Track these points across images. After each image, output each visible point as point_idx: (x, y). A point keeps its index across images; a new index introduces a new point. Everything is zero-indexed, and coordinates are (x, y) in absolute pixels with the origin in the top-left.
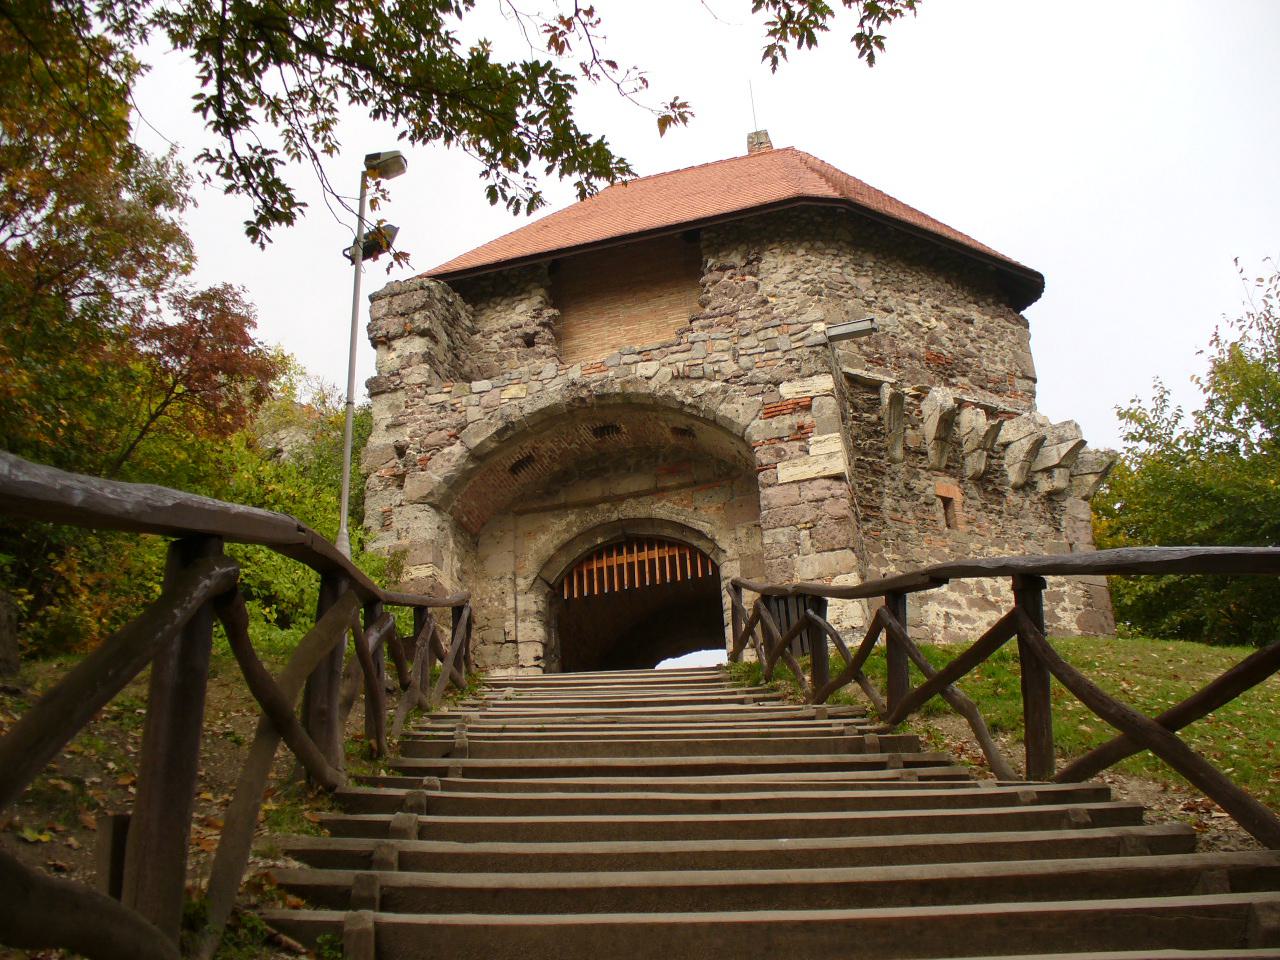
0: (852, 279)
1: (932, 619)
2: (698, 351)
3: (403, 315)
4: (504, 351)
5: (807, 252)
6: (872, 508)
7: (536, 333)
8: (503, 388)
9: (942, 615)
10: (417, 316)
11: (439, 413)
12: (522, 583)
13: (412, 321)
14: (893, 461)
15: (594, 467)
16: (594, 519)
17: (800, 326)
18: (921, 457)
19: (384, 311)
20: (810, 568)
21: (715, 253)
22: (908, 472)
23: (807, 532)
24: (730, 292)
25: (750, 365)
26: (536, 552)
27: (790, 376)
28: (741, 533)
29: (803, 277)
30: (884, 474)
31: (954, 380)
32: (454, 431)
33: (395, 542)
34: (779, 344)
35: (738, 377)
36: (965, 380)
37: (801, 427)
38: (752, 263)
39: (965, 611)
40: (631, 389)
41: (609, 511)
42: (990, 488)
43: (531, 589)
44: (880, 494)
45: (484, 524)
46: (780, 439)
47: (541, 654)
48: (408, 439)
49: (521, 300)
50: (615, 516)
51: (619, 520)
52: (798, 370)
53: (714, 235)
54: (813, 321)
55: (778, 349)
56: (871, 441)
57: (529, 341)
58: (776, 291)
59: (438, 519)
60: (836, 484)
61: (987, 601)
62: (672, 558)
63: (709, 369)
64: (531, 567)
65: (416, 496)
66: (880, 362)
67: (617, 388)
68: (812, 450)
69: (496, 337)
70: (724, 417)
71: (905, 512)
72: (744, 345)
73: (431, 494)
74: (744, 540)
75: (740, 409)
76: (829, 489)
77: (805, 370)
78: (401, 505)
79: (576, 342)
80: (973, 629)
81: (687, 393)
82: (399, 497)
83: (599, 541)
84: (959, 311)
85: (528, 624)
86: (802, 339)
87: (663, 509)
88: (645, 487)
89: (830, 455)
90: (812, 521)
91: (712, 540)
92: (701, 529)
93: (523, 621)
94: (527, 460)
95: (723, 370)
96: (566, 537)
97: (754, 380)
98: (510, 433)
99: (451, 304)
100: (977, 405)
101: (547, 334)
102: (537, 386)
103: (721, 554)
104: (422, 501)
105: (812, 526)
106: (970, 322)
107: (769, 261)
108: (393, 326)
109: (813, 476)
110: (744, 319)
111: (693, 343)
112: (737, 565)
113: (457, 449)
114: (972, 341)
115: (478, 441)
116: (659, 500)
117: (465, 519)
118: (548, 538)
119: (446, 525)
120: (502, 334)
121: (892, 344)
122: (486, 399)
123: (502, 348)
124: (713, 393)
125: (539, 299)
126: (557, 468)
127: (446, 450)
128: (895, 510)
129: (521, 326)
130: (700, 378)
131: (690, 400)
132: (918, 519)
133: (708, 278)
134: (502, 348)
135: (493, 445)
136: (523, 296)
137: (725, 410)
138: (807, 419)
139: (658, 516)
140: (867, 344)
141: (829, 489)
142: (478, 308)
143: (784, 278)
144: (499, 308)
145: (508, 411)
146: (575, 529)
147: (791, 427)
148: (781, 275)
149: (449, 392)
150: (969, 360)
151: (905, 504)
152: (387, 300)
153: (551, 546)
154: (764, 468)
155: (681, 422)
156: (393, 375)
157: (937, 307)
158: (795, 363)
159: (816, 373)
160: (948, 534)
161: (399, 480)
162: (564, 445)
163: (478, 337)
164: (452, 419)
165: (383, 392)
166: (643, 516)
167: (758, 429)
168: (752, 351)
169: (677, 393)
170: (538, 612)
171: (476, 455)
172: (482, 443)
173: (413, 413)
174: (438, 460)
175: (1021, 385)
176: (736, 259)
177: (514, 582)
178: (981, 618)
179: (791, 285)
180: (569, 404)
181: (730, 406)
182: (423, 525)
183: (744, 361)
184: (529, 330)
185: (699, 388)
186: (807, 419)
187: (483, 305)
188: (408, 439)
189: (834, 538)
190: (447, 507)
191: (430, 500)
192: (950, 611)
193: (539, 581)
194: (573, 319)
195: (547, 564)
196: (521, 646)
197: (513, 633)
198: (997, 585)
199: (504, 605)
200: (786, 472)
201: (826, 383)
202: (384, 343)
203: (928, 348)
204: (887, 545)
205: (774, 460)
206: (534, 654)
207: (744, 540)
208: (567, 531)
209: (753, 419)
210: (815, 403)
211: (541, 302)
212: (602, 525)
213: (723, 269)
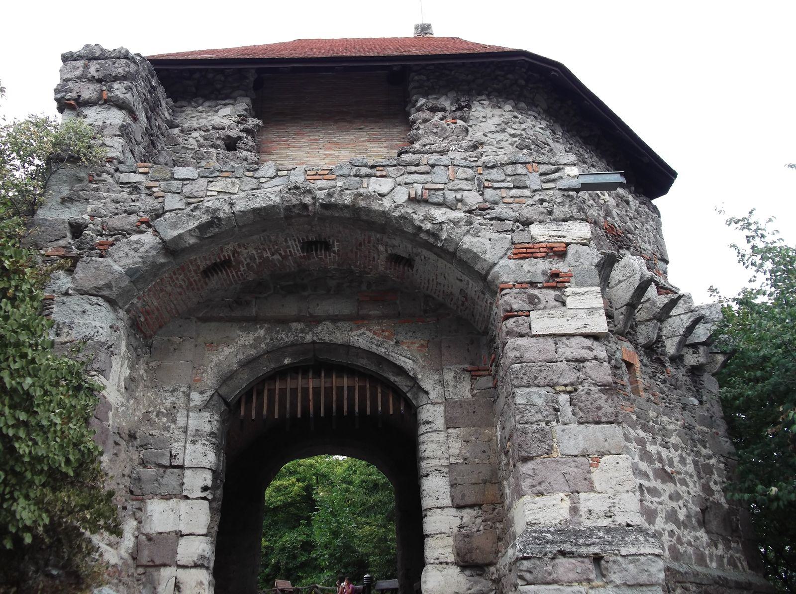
2: (440, 175)
3: (99, 81)
4: (202, 149)
7: (240, 138)
10: (116, 85)
11: (130, 193)
12: (197, 398)
13: (110, 89)
15: (291, 283)
16: (285, 337)
19: (78, 73)
20: (572, 442)
21: (426, 95)
23: (567, 396)
24: (440, 133)
25: (497, 198)
26: (216, 365)
27: (541, 218)
28: (449, 376)
32: (146, 217)
34: (528, 183)
35: (484, 209)
37: (556, 275)
38: (462, 108)
40: (362, 204)
41: (302, 331)
43: (206, 406)
45: (160, 327)
46: (533, 284)
47: (209, 483)
48: (86, 217)
49: (225, 105)
50: (309, 338)
51: (314, 342)
53: (424, 78)
54: (565, 164)
55: (526, 187)
58: (484, 139)
59: (112, 316)
60: (596, 345)
61: (666, 472)
62: (362, 389)
64: (209, 379)
65: (88, 286)
67: (347, 199)
68: (569, 301)
69: (195, 134)
70: (468, 251)
73: (108, 286)
74: (452, 384)
75: (486, 244)
77: (558, 212)
78: (66, 294)
80: (660, 503)
81: (425, 218)
83: (286, 362)
85: (199, 447)
87: (363, 338)
88: (346, 311)
89: (591, 311)
90: (572, 384)
91: (414, 379)
92: (402, 364)
93: (193, 442)
94: (223, 265)
95: (467, 200)
96: (253, 352)
97: (503, 216)
99: (154, 88)
102: (253, 183)
103: (421, 395)
104: (95, 292)
105: (572, 390)
108: (88, 92)
109: (573, 331)
111: (433, 166)
112: (440, 409)
114: (631, 219)
115: (176, 233)
116: (359, 328)
117: (142, 319)
118: (232, 351)
119: (120, 324)
120: (203, 133)
123: (200, 146)
124: (456, 223)
125: (245, 106)
126: (251, 277)
127: (134, 238)
129: (223, 129)
130: (439, 205)
131: (428, 226)
134: (200, 146)
135: (192, 241)
136: (227, 101)
137: (468, 242)
139: (356, 345)
141: (591, 349)
142: (179, 104)
143: (493, 128)
144: (200, 108)
146: (263, 346)
147: (544, 273)
149: (146, 173)
153: (235, 361)
154: (510, 314)
155: (403, 248)
158: (545, 204)
159: (572, 218)
160: (634, 400)
162: (266, 254)
163: (176, 131)
164: (146, 203)
166: (340, 341)
167: (507, 270)
168: (496, 185)
170: (212, 434)
171: (170, 249)
172: (180, 236)
173: (97, 190)
174: (122, 246)
175: (660, 264)
179: (500, 136)
181: (476, 240)
183: (489, 193)
184: (234, 133)
186: (561, 267)
187: (183, 103)
188: (86, 217)
190: (125, 303)
191: (106, 293)
192: (643, 482)
193: (216, 397)
194: (272, 136)
195: (226, 379)
196: (188, 473)
197: (180, 457)
200: (540, 323)
201: (581, 230)
202: (72, 108)
203: (605, 218)
205: (527, 307)
206: (202, 484)
207: (452, 384)
209: (501, 258)
210: (571, 250)
211: (246, 110)
212: (293, 345)
213: (434, 110)
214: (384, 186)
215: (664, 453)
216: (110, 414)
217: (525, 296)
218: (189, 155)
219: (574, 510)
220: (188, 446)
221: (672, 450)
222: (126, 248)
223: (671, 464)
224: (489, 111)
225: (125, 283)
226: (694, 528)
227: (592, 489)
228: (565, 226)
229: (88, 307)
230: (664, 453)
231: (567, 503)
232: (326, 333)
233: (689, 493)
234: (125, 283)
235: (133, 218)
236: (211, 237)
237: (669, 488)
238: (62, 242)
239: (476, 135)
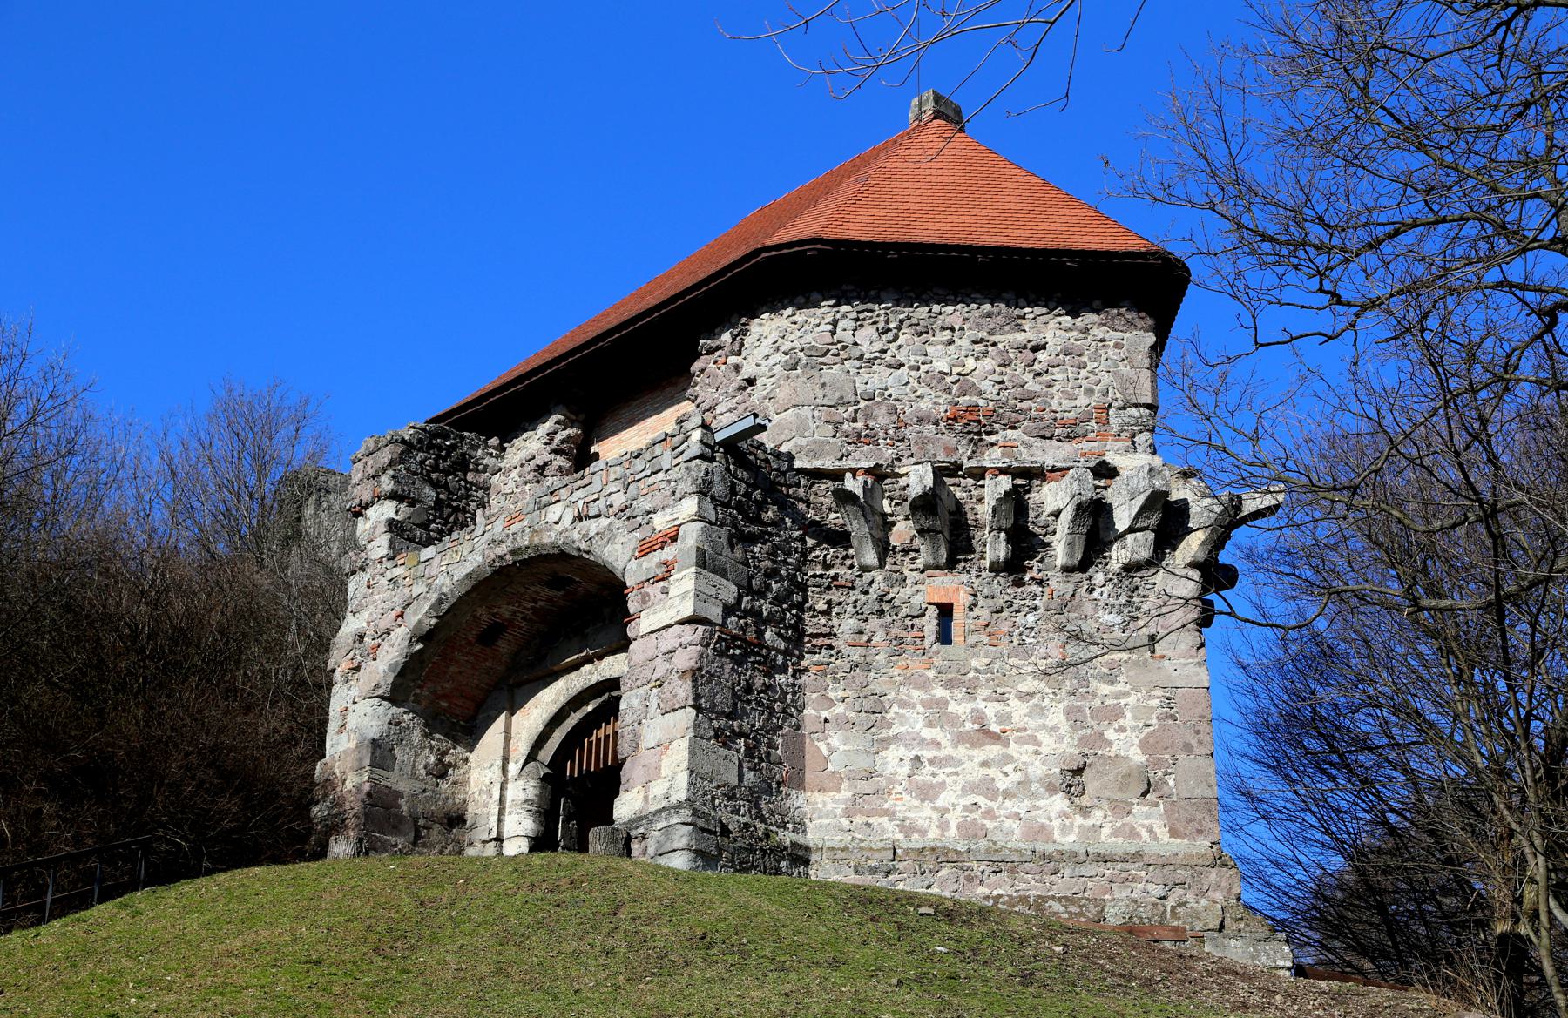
18: (913, 555)
29: (786, 346)
31: (993, 438)
39: (948, 751)
66: (872, 439)
69: (514, 474)
73: (377, 687)
101: (560, 461)
133: (695, 367)
150: (1026, 404)
162: (530, 605)
167: (633, 573)
178: (971, 758)
185: (593, 527)
191: (380, 692)
198: (1007, 709)
204: (836, 680)
213: (711, 351)
215: (991, 710)
216: (402, 802)
219: (646, 798)
221: (1014, 702)
223: (1004, 718)
226: (1034, 795)
230: (991, 710)
233: (1037, 753)
237: (993, 751)
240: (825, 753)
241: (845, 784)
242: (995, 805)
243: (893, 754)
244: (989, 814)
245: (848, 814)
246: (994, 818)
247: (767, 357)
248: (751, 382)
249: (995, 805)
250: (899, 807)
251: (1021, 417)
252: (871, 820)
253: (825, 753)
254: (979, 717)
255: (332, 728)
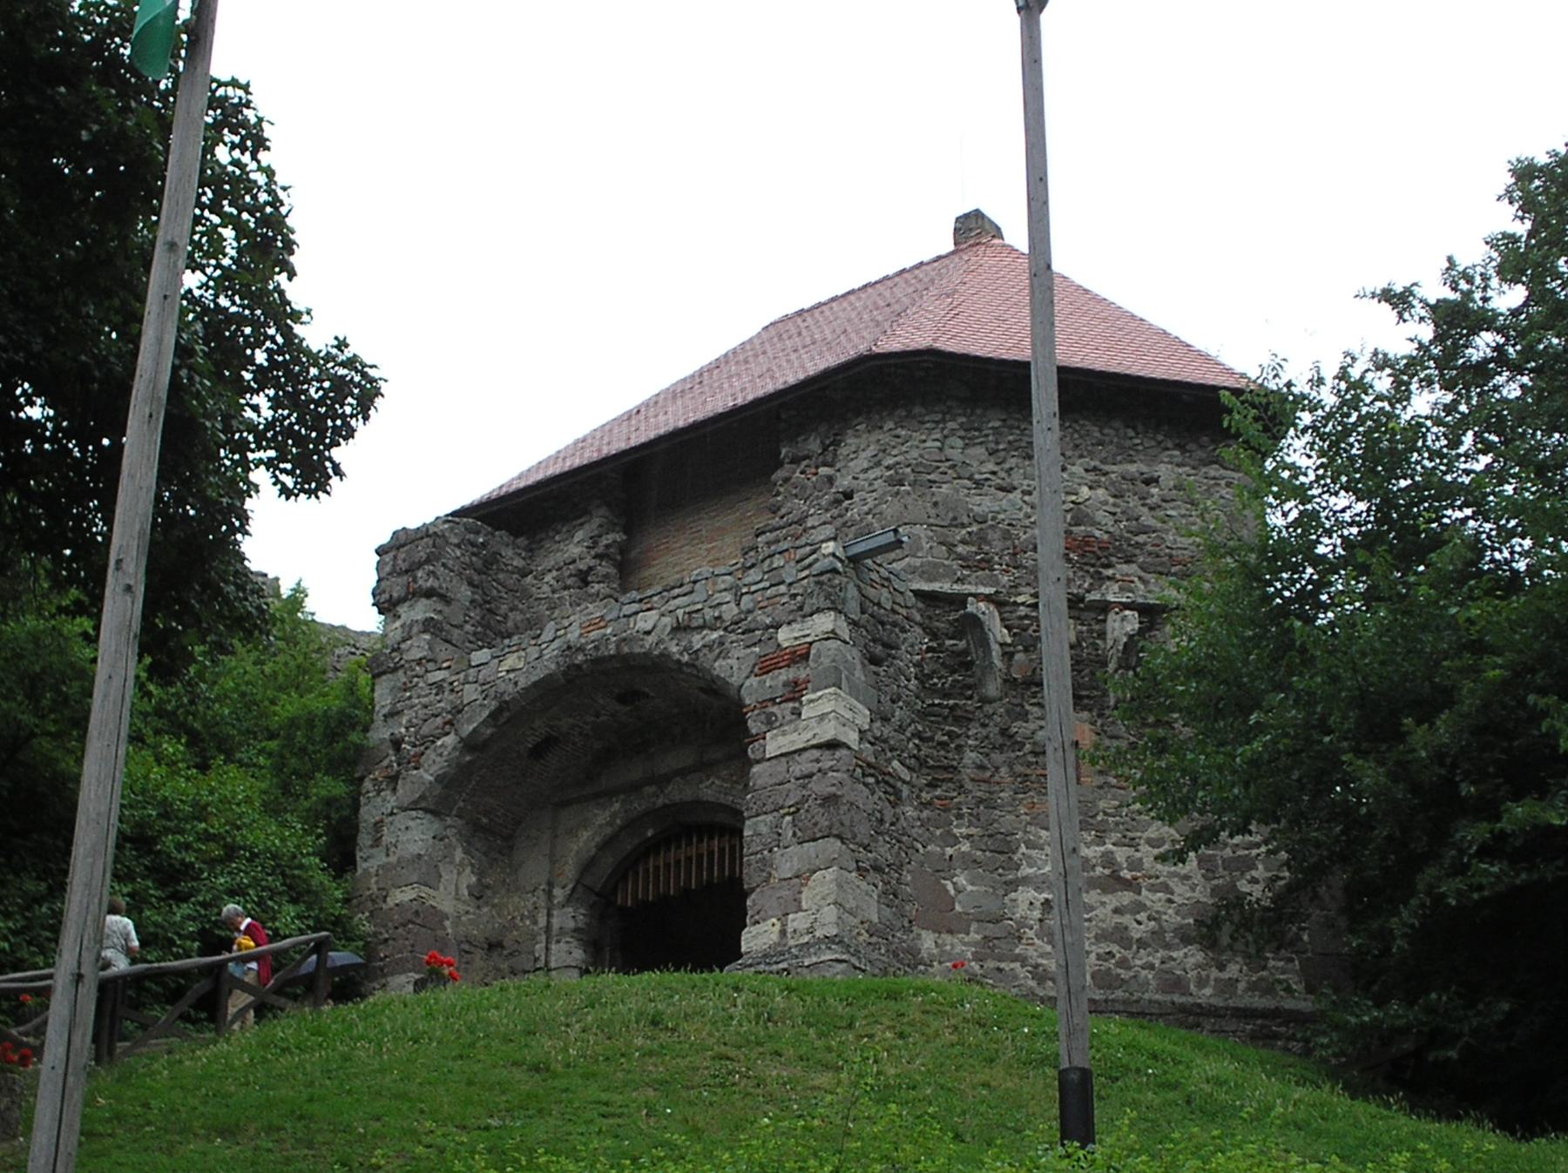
0: (955, 454)
1: (1021, 910)
3: (407, 571)
5: (899, 425)
6: (945, 768)
7: (591, 568)
8: (500, 658)
9: (1038, 904)
10: (420, 574)
14: (985, 700)
16: (639, 806)
17: (808, 549)
18: (1034, 689)
22: (1007, 711)
29: (890, 461)
30: (970, 720)
31: (1110, 572)
33: (385, 859)
36: (1132, 568)
40: (626, 650)
42: (1151, 720)
43: (569, 900)
44: (959, 748)
50: (660, 802)
51: (665, 806)
52: (801, 608)
55: (783, 582)
56: (956, 676)
57: (584, 578)
59: (437, 825)
61: (1120, 879)
63: (709, 614)
64: (570, 871)
66: (986, 565)
69: (548, 578)
71: (997, 769)
72: (747, 580)
73: (423, 797)
76: (818, 761)
77: (807, 609)
78: (392, 814)
79: (653, 571)
82: (392, 801)
83: (650, 834)
84: (1132, 468)
86: (810, 565)
89: (822, 717)
96: (609, 831)
97: (753, 626)
98: (508, 715)
100: (1126, 606)
101: (605, 568)
104: (413, 806)
106: (1151, 481)
107: (851, 441)
110: (813, 527)
111: (695, 582)
113: (450, 740)
117: (485, 820)
118: (586, 834)
120: (555, 573)
121: (1006, 536)
122: (485, 671)
127: (439, 743)
128: (982, 767)
129: (574, 561)
131: (686, 658)
132: (1015, 775)
133: (779, 474)
134: (554, 592)
137: (720, 667)
138: (801, 673)
140: (963, 542)
141: (818, 761)
143: (865, 465)
145: (502, 687)
147: (785, 684)
148: (862, 462)
150: (1141, 538)
151: (997, 757)
152: (391, 555)
156: (393, 650)
157: (1095, 469)
161: (393, 779)
162: (591, 719)
164: (446, 702)
165: (384, 673)
166: (689, 799)
167: (753, 690)
168: (753, 588)
169: (675, 649)
170: (576, 930)
171: (468, 744)
173: (410, 698)
174: (431, 754)
176: (814, 445)
177: (549, 895)
178: (1103, 904)
179: (871, 475)
180: (564, 674)
182: (414, 835)
184: (582, 566)
185: (697, 641)
189: (816, 824)
190: (451, 809)
193: (580, 889)
195: (587, 867)
198: (1138, 855)
199: (535, 923)
200: (775, 744)
201: (825, 622)
204: (959, 816)
208: (609, 824)
213: (796, 461)
214: (645, 621)
215: (1121, 854)
216: (447, 923)
217: (763, 717)
218: (543, 608)
219: (783, 933)
220: (553, 946)
221: (1145, 848)
222: (433, 756)
223: (1135, 865)
224: (863, 442)
225: (438, 790)
226: (1168, 946)
227: (800, 909)
228: (809, 622)
229: (411, 823)
230: (1121, 854)
231: (778, 926)
232: (678, 792)
233: (1170, 901)
234: (438, 790)
235: (439, 721)
236: (509, 720)
237: (1126, 897)
238: (385, 763)
239: (844, 482)
240: (952, 892)
241: (974, 926)
242: (1128, 954)
243: (1025, 895)
244: (1124, 963)
245: (978, 958)
246: (1129, 968)
247: (865, 471)
248: (848, 495)
249: (1128, 954)
250: (1031, 952)
251: (1137, 552)
252: (1002, 965)
253: (952, 892)
254: (1108, 860)
255: (364, 839)
